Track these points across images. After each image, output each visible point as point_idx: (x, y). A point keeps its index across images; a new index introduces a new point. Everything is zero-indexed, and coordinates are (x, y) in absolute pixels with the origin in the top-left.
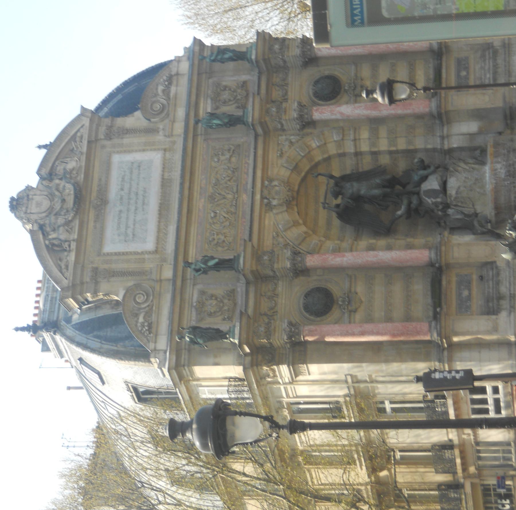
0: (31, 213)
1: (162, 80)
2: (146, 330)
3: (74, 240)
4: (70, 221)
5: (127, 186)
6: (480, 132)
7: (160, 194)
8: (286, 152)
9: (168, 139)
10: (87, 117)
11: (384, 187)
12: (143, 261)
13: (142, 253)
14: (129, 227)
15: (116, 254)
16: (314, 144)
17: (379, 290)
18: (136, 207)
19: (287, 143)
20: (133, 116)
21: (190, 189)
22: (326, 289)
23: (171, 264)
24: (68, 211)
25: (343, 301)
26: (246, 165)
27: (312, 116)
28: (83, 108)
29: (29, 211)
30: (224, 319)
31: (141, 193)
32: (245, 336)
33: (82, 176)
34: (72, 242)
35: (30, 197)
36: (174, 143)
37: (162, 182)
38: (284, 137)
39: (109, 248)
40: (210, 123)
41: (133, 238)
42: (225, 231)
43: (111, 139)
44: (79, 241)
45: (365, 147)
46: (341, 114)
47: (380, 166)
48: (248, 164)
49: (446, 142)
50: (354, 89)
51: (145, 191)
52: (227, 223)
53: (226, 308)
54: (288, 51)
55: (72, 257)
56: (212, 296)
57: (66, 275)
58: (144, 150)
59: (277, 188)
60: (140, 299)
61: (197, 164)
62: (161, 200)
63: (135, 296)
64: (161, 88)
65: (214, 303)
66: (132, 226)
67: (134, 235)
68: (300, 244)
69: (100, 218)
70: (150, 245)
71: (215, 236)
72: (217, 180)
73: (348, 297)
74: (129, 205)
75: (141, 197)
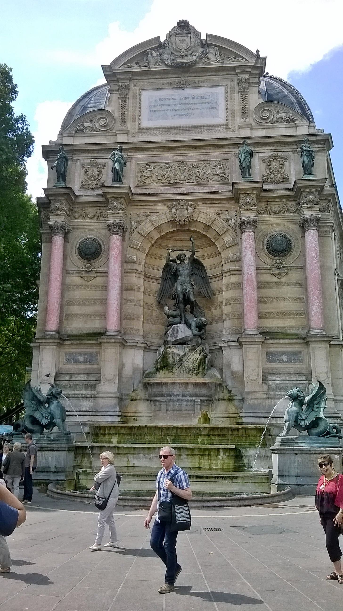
0: (176, 37)
1: (291, 115)
2: (78, 128)
3: (149, 68)
4: (165, 64)
5: (195, 101)
6: (233, 373)
9: (236, 126)
11: (184, 295)
12: (134, 120)
13: (140, 119)
15: (140, 100)
16: (227, 239)
17: (97, 294)
18: (178, 110)
19: (228, 217)
20: (259, 98)
21: (190, 147)
24: (173, 60)
25: (88, 267)
27: (244, 232)
28: (265, 59)
30: (82, 182)
31: (190, 112)
32: (51, 193)
33: (204, 67)
34: (148, 67)
36: (234, 131)
37: (198, 127)
38: (234, 214)
39: (145, 95)
40: (242, 152)
41: (152, 111)
42: (154, 177)
43: (238, 83)
44: (149, 73)
45: (225, 280)
46: (245, 256)
47: (213, 295)
48: (212, 189)
49: (226, 345)
50: (277, 268)
51: (191, 114)
53: (90, 182)
54: (309, 208)
55: (136, 69)
56: (100, 172)
59: (186, 212)
60: (102, 122)
61: (213, 151)
62: (183, 127)
63: (104, 118)
64: (283, 115)
65: (94, 174)
66: (161, 109)
67: (155, 111)
69: (171, 86)
70: (145, 124)
71: (149, 170)
72: (197, 167)
73: (91, 271)
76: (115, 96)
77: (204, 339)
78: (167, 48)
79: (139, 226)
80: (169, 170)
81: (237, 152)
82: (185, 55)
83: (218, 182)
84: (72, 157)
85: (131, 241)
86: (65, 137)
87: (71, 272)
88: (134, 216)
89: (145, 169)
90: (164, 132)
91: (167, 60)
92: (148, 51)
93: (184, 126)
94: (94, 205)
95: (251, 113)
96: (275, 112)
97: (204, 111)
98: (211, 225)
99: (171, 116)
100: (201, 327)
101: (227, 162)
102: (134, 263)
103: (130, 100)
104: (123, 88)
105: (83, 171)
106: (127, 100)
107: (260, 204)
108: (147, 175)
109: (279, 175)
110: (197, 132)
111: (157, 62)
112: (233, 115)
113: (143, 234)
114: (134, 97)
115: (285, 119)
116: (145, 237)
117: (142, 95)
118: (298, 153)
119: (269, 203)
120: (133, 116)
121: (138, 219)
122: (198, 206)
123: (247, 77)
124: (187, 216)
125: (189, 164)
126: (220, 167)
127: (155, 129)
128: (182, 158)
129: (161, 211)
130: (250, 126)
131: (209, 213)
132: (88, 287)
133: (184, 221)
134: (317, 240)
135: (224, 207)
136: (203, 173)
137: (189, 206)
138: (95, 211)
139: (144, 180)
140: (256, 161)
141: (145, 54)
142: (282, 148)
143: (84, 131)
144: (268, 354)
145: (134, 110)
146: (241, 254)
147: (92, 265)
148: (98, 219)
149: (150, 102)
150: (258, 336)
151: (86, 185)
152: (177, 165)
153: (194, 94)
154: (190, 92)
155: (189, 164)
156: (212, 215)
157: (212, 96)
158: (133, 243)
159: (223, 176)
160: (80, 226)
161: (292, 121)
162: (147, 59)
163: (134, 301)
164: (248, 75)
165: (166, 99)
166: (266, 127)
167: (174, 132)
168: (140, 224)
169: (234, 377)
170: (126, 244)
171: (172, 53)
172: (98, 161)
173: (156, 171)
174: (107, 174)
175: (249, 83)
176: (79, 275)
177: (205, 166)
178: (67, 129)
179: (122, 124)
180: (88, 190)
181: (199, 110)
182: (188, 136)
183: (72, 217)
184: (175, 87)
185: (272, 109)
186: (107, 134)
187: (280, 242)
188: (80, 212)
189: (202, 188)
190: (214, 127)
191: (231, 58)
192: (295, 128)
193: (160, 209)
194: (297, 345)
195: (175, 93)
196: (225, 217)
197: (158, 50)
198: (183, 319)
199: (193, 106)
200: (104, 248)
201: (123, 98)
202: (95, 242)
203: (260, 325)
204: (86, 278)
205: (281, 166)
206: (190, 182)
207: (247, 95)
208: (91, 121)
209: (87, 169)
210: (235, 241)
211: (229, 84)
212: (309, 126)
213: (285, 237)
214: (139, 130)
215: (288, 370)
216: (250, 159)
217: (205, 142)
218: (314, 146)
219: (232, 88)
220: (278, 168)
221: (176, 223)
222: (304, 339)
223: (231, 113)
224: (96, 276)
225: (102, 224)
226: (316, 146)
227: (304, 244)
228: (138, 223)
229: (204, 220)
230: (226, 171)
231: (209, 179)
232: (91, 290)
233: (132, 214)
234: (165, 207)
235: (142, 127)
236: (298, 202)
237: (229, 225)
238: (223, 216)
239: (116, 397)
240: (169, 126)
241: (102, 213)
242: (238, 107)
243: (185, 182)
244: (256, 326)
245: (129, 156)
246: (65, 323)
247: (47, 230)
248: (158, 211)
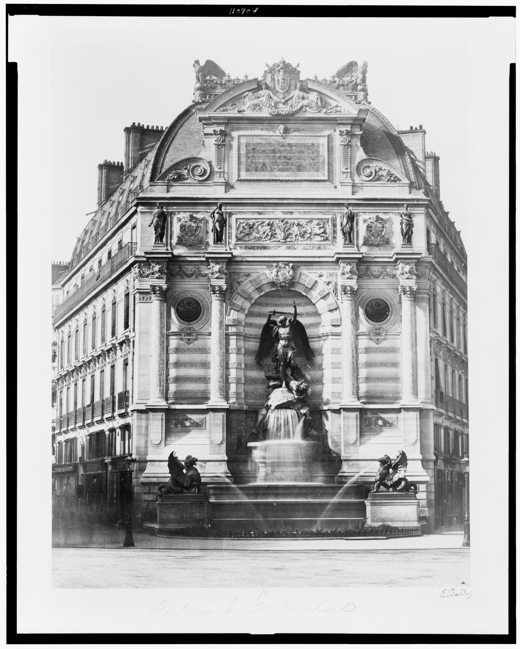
10: (358, 114)
26: (311, 248)
55: (233, 113)
57: (218, 110)
122: (299, 267)
132: (189, 349)
139: (243, 237)
155: (290, 221)
161: (394, 179)
164: (350, 126)
176: (179, 337)
198: (284, 383)
214: (237, 181)
224: (197, 339)
233: (232, 274)
234: (265, 267)
235: (240, 178)
238: (324, 279)
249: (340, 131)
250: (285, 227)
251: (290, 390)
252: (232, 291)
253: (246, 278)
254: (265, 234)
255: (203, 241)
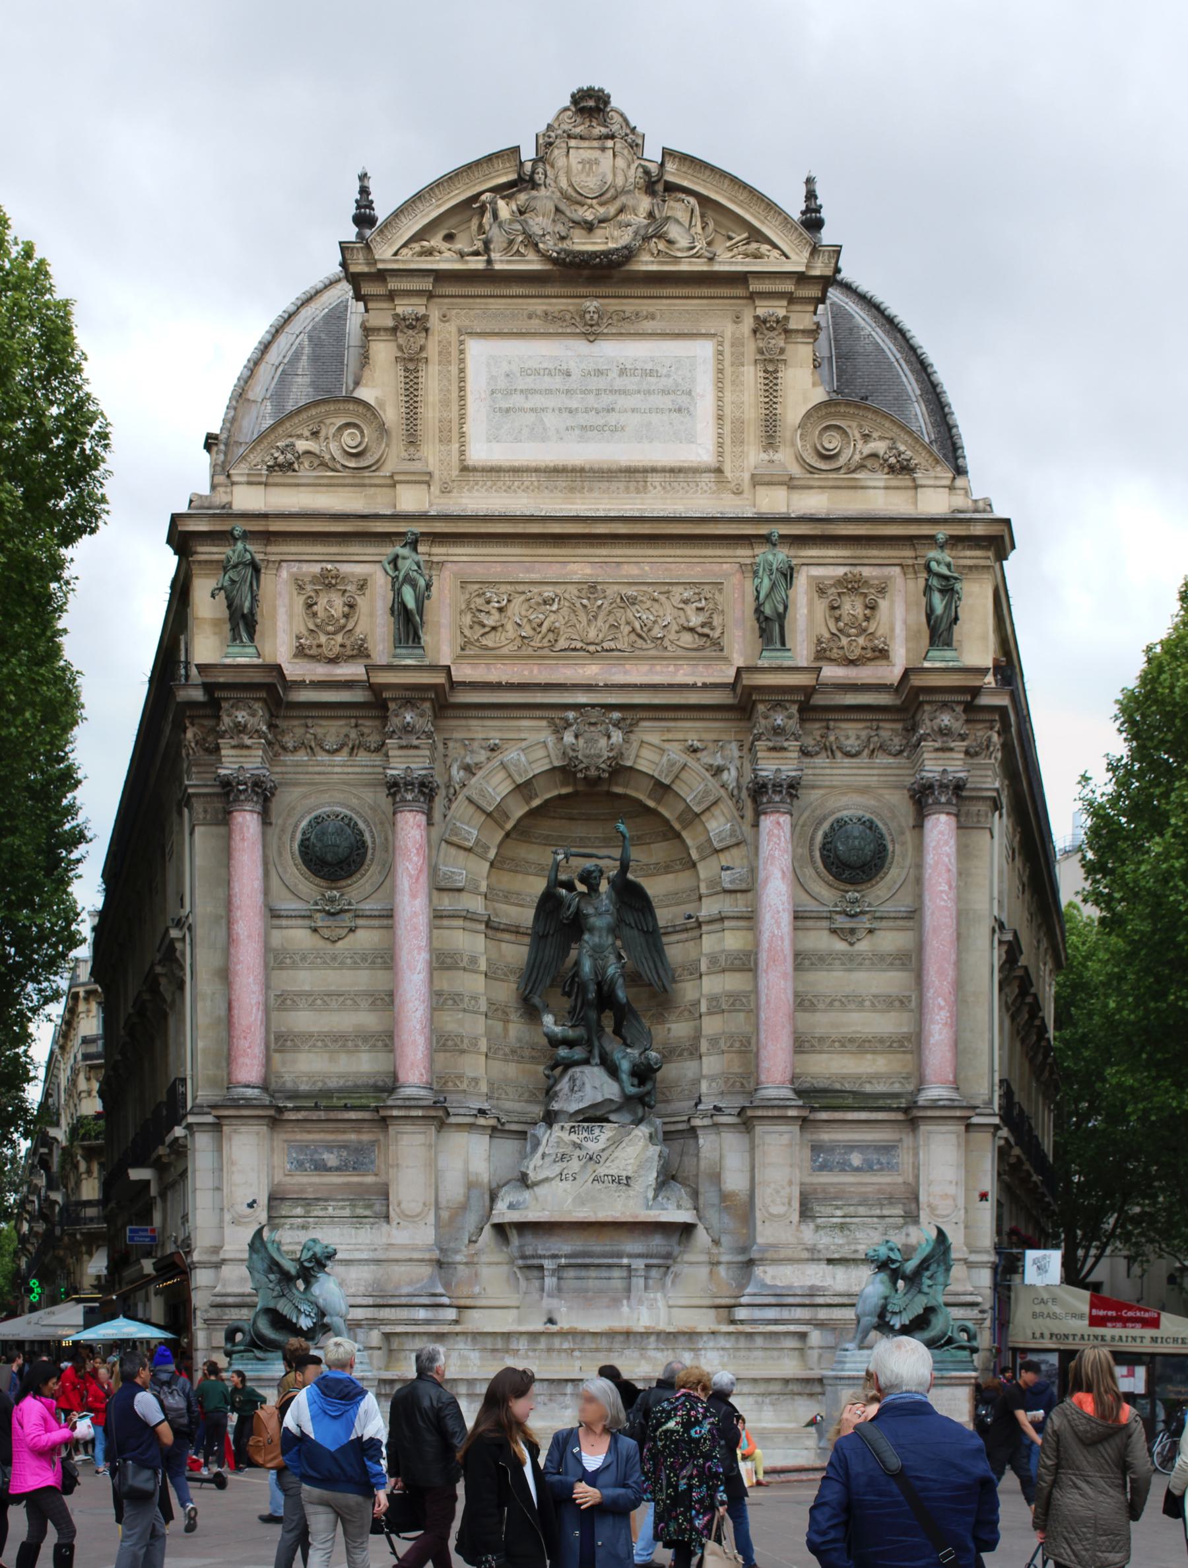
0: (568, 149)
1: (902, 448)
4: (538, 251)
7: (605, 466)
8: (699, 759)
9: (746, 476)
12: (445, 440)
13: (462, 435)
14: (527, 398)
15: (462, 371)
18: (577, 409)
19: (718, 761)
20: (814, 385)
22: (362, 864)
23: (431, 505)
24: (563, 238)
25: (332, 900)
29: (573, 143)
30: (298, 638)
33: (654, 268)
35: (610, 143)
36: (738, 492)
38: (736, 753)
39: (476, 350)
42: (510, 627)
43: (755, 332)
44: (489, 277)
48: (677, 671)
51: (615, 429)
52: (527, 631)
55: (446, 261)
58: (720, 418)
61: (679, 552)
62: (592, 470)
66: (528, 405)
67: (508, 410)
68: (470, 800)
70: (480, 452)
71: (497, 605)
72: (633, 601)
73: (342, 911)
74: (582, 392)
75: (599, 420)
76: (383, 351)
77: (651, 1107)
78: (543, 188)
79: (470, 779)
80: (555, 607)
81: (748, 561)
82: (601, 221)
83: (693, 654)
84: (265, 554)
85: (450, 826)
86: (237, 483)
87: (283, 913)
88: (454, 749)
89: (480, 601)
90: (536, 484)
91: (544, 235)
92: (483, 197)
93: (596, 466)
94: (341, 713)
95: (788, 434)
96: (858, 436)
97: (655, 418)
98: (673, 782)
99: (558, 432)
100: (644, 1073)
101: (720, 591)
102: (460, 890)
103: (430, 368)
104: (411, 327)
105: (300, 601)
106: (422, 366)
107: (808, 726)
108: (490, 621)
109: (861, 641)
110: (632, 488)
111: (511, 242)
112: (738, 441)
113: (484, 804)
114: (444, 354)
115: (886, 460)
116: (489, 815)
117: (467, 351)
118: (915, 573)
119: (832, 724)
120: (440, 421)
121: (468, 760)
122: (636, 724)
123: (781, 313)
124: (606, 754)
125: (611, 591)
126: (700, 605)
127: (509, 471)
128: (588, 571)
129: (533, 737)
130: (787, 479)
131: (666, 746)
133: (598, 768)
134: (952, 842)
135: (707, 730)
136: (650, 624)
137: (615, 725)
138: (345, 730)
139: (482, 635)
140: (801, 591)
141: (471, 207)
142: (875, 553)
143: (296, 466)
144: (816, 1148)
145: (445, 403)
146: (753, 871)
147: (342, 895)
148: (351, 754)
149: (493, 378)
150: (793, 1103)
151: (310, 647)
152: (576, 592)
153: (622, 361)
154: (611, 350)
155: (611, 591)
156: (676, 753)
157: (677, 369)
158: (455, 831)
159: (707, 636)
160: (301, 776)
162: (481, 226)
163: (462, 1000)
164: (785, 303)
165: (542, 372)
166: (831, 483)
167: (564, 484)
168: (474, 774)
169: (727, 1207)
170: (436, 832)
171: (557, 210)
172: (345, 568)
173: (517, 608)
174: (372, 615)
175: (787, 332)
177: (655, 600)
178: (243, 458)
179: (412, 449)
180: (319, 661)
181: (636, 419)
182: (606, 501)
183: (277, 747)
184: (569, 331)
185: (849, 423)
186: (367, 481)
187: (856, 842)
188: (299, 731)
189: (646, 668)
190: (682, 475)
191: (738, 238)
192: (911, 493)
193: (531, 729)
194: (888, 1125)
195: (569, 353)
196: (711, 762)
197: (513, 194)
199: (623, 402)
200: (374, 842)
201: (411, 360)
202: (348, 825)
203: (798, 1070)
204: (326, 933)
205: (867, 612)
206: (612, 650)
207: (779, 375)
208: (315, 434)
209: (313, 594)
210: (738, 833)
211: (729, 329)
212: (951, 488)
213: (870, 828)
215: (864, 1189)
216: (786, 590)
217: (656, 525)
218: (962, 554)
219: (737, 343)
220: (861, 617)
221: (575, 774)
222: (906, 1110)
223: (732, 432)
225: (366, 770)
226: (968, 553)
227: (920, 848)
228: (469, 769)
229: (654, 767)
230: (716, 621)
231: (666, 643)
232: (342, 966)
233: (451, 744)
234: (544, 723)
236: (909, 723)
237: (723, 786)
238: (705, 758)
239: (430, 1260)
240: (552, 464)
241: (362, 735)
242: (753, 410)
243: (599, 649)
244: (788, 1076)
245: (435, 559)
246: (277, 1057)
247: (206, 786)
248: (523, 736)
249: (757, 318)
250: (599, 607)
251: (613, 1071)
252: (452, 791)
253: (489, 753)
254: (544, 629)
255: (366, 649)
